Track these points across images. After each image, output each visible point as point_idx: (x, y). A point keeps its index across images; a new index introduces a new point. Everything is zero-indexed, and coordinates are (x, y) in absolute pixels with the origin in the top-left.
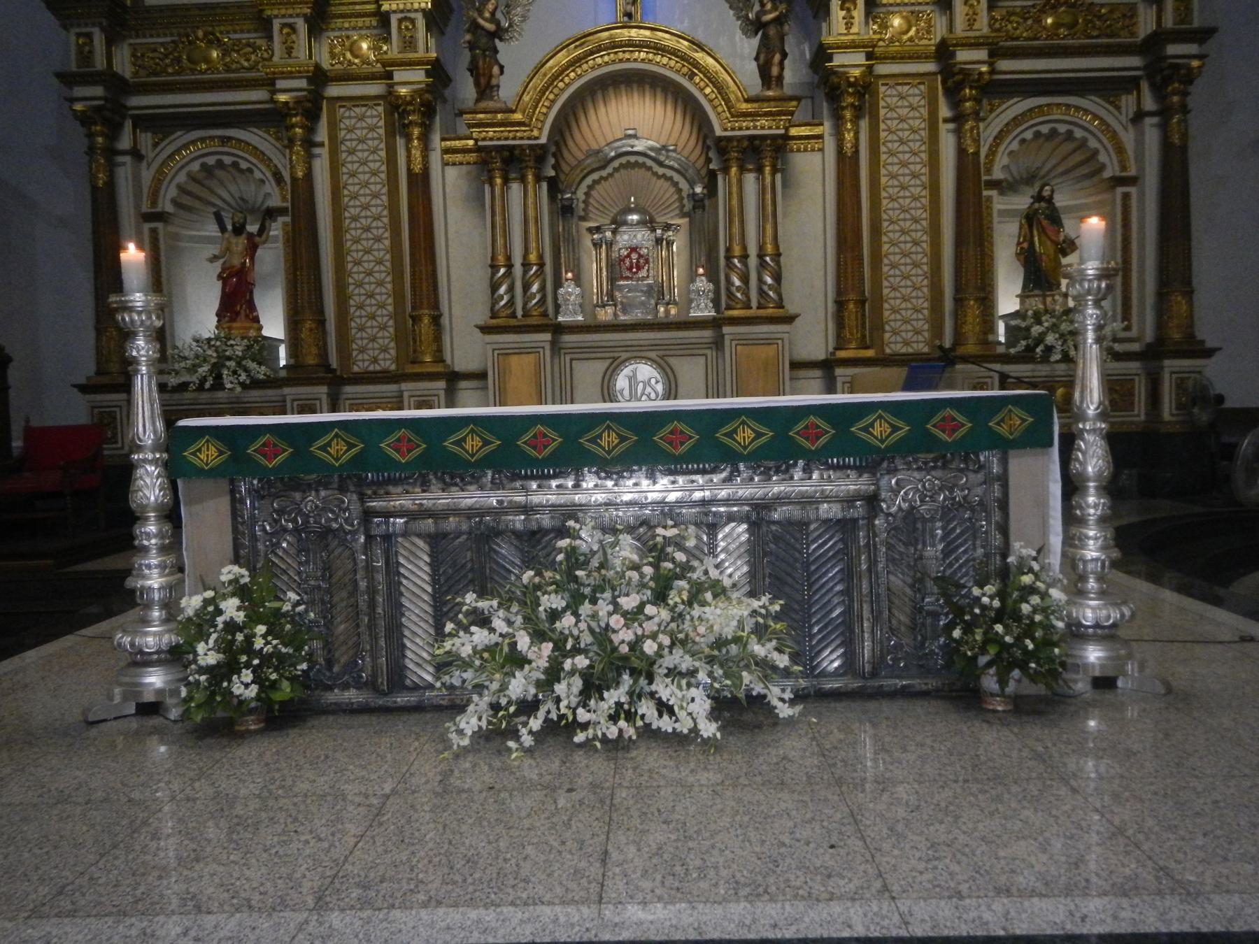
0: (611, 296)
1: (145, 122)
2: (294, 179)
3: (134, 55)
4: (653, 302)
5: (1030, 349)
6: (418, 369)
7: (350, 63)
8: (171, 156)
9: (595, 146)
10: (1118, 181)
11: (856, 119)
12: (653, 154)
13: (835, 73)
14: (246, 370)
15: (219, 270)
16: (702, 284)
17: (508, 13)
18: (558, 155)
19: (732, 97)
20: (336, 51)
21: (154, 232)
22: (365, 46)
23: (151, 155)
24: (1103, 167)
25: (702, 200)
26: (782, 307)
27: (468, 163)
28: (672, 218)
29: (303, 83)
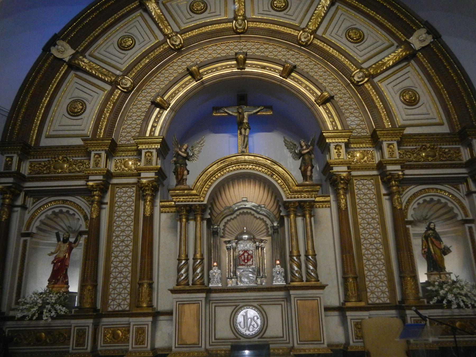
0: (235, 273)
1: (29, 193)
2: (92, 219)
3: (30, 166)
4: (255, 277)
5: (440, 302)
6: (139, 311)
7: (123, 170)
8: (39, 208)
9: (228, 205)
11: (345, 194)
12: (254, 209)
13: (335, 175)
14: (56, 310)
15: (53, 259)
16: (278, 268)
17: (192, 150)
18: (212, 209)
19: (291, 184)
20: (118, 165)
21: (25, 241)
22: (130, 163)
23: (31, 207)
24: (456, 215)
25: (277, 229)
26: (318, 281)
27: (172, 212)
28: (263, 237)
29: (101, 178)
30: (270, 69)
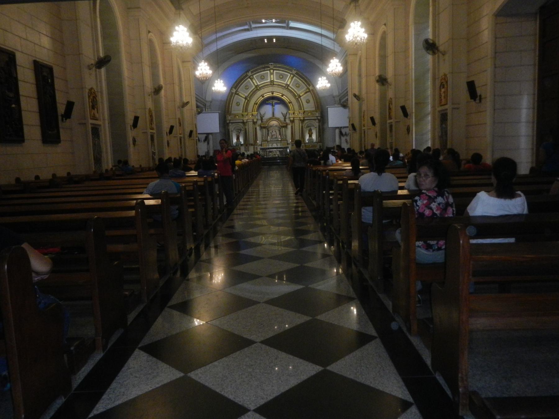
1: (231, 123)
10: (316, 128)
30: (279, 95)
